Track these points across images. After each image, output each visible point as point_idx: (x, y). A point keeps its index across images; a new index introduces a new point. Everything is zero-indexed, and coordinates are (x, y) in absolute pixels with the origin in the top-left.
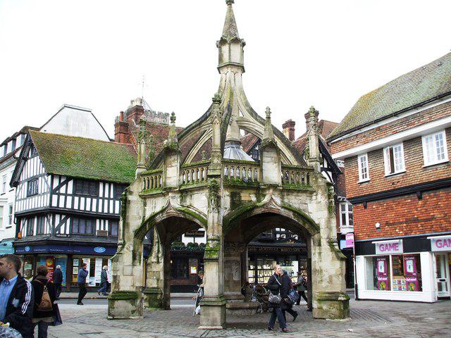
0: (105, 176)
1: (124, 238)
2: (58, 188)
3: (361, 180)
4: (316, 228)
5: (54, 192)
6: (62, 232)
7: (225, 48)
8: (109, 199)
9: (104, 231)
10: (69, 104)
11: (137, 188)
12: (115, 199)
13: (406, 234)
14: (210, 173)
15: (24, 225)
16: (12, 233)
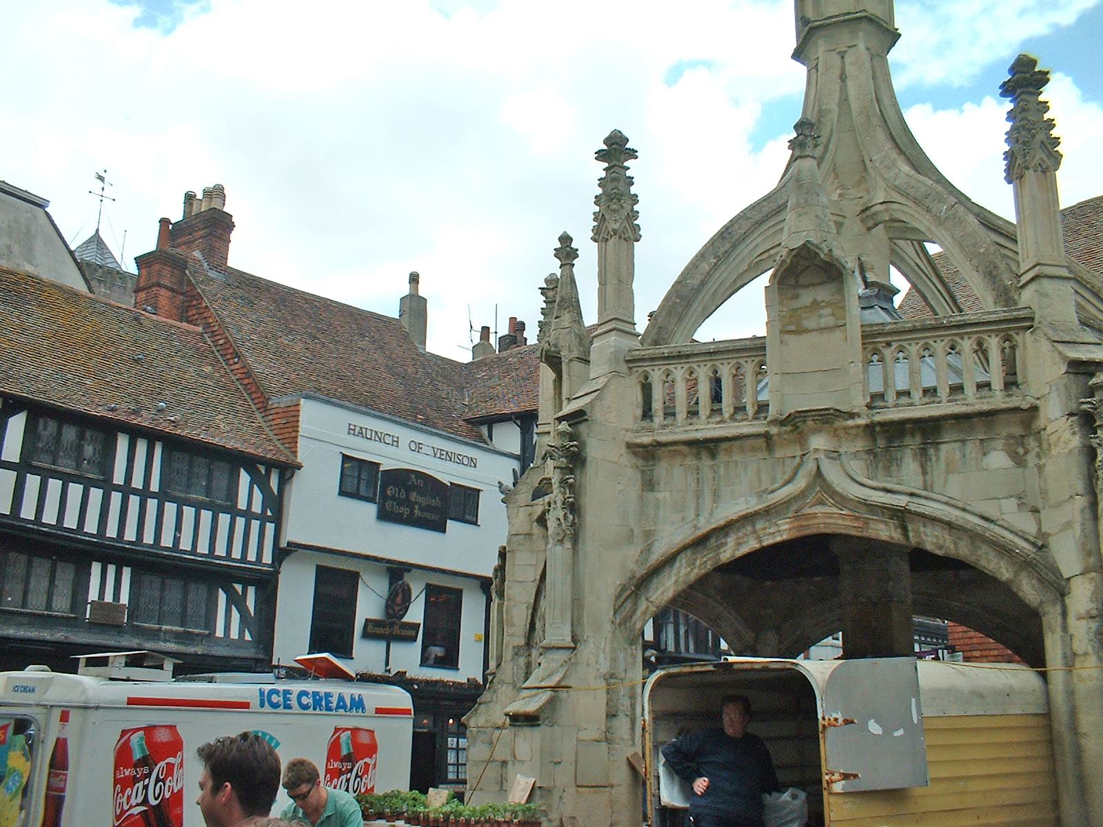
0: (144, 420)
1: (576, 623)
8: (144, 494)
9: (115, 607)
12: (163, 497)
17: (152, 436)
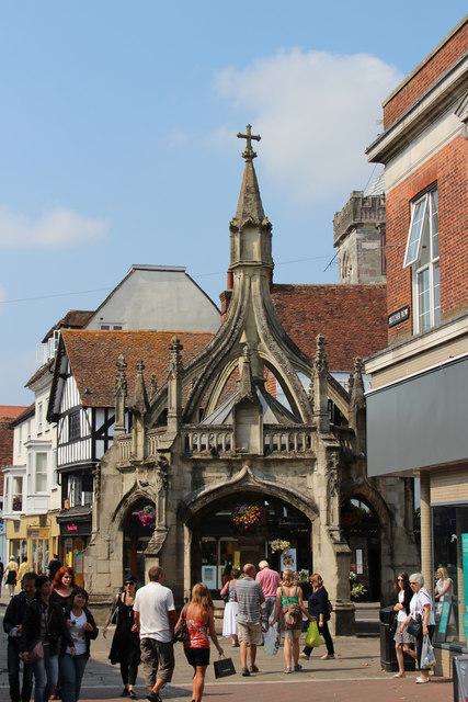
2: (105, 428)
4: (316, 510)
10: (141, 262)
16: (55, 502)
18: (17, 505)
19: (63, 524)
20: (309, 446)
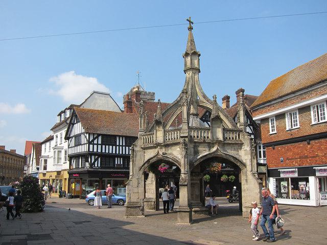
3: (271, 133)
4: (245, 165)
5: (90, 143)
6: (96, 166)
7: (189, 59)
8: (122, 146)
9: (120, 165)
11: (140, 143)
12: (125, 146)
13: (300, 165)
14: (182, 135)
15: (74, 161)
16: (67, 166)
17: (123, 136)
18: (45, 168)
19: (70, 174)
20: (239, 138)
